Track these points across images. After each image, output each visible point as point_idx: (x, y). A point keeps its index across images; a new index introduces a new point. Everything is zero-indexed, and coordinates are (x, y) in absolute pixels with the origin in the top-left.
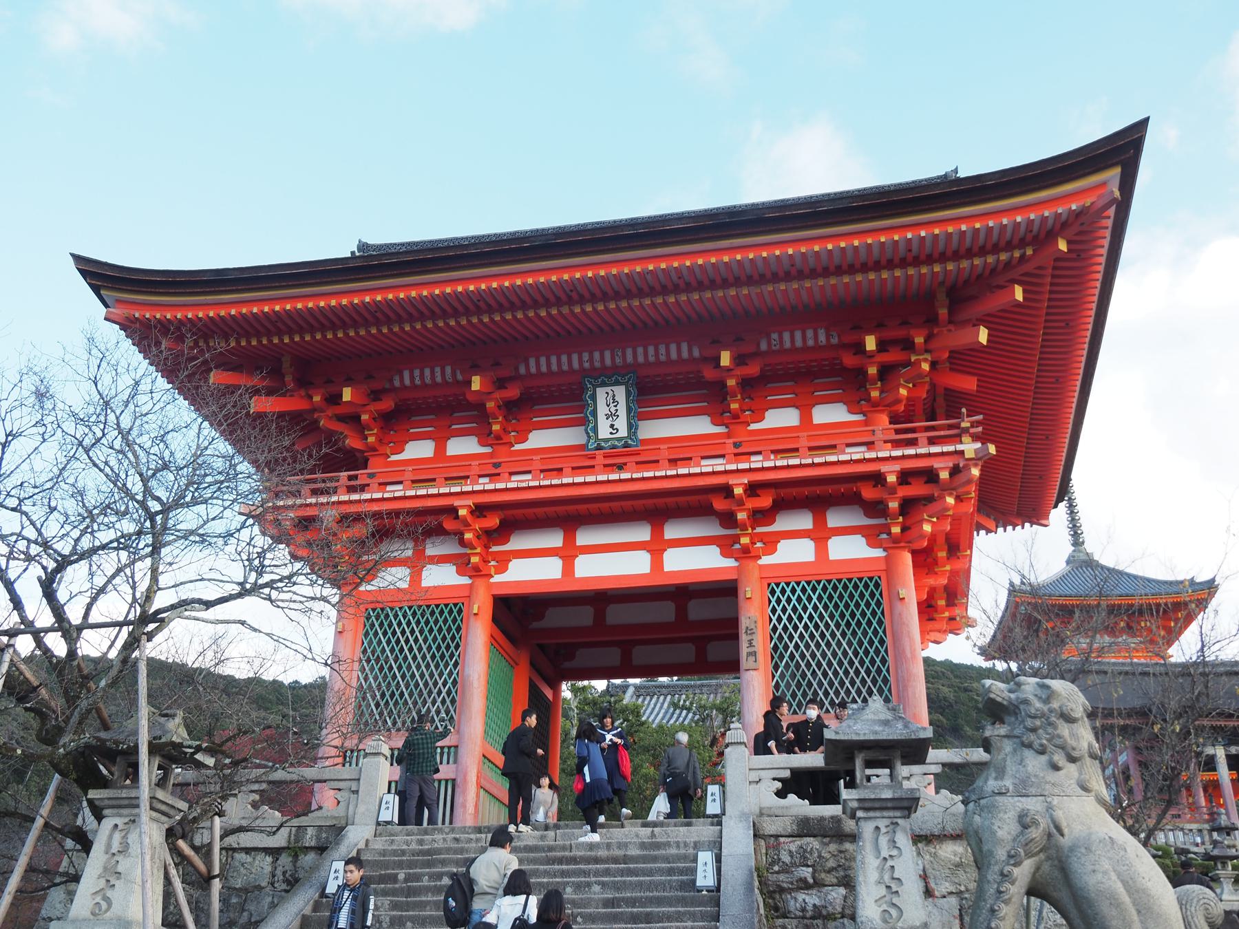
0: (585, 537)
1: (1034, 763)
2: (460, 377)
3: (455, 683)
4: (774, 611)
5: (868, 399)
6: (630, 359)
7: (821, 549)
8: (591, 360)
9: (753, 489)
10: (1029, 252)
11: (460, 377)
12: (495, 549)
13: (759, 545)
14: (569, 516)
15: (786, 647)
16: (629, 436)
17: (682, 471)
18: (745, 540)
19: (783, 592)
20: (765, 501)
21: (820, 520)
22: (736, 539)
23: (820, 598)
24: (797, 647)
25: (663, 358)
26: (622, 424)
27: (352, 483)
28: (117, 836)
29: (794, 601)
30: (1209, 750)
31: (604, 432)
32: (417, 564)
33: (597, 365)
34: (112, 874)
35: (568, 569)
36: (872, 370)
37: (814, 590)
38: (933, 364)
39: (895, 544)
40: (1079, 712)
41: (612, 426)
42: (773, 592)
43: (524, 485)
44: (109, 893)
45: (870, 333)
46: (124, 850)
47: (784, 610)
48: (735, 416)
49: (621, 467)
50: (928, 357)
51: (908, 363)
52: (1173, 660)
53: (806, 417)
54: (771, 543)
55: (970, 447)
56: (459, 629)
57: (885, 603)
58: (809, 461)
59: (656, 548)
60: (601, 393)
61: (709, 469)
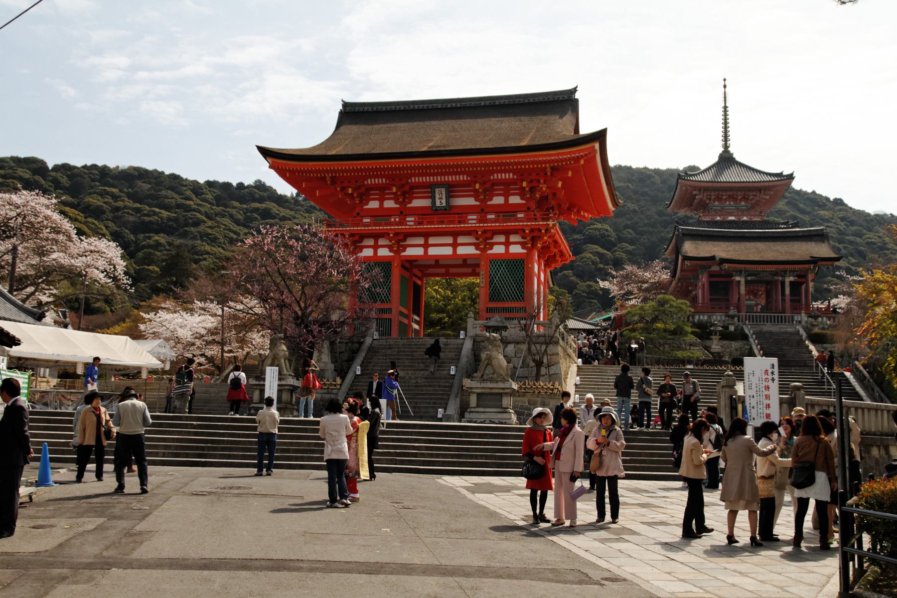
0: (432, 241)
1: (490, 347)
7: (507, 249)
9: (485, 232)
14: (426, 235)
20: (489, 235)
21: (507, 239)
26: (444, 201)
30: (738, 278)
31: (438, 204)
32: (376, 247)
34: (320, 352)
35: (426, 251)
38: (548, 187)
49: (442, 223)
54: (491, 246)
59: (455, 245)
60: (437, 190)
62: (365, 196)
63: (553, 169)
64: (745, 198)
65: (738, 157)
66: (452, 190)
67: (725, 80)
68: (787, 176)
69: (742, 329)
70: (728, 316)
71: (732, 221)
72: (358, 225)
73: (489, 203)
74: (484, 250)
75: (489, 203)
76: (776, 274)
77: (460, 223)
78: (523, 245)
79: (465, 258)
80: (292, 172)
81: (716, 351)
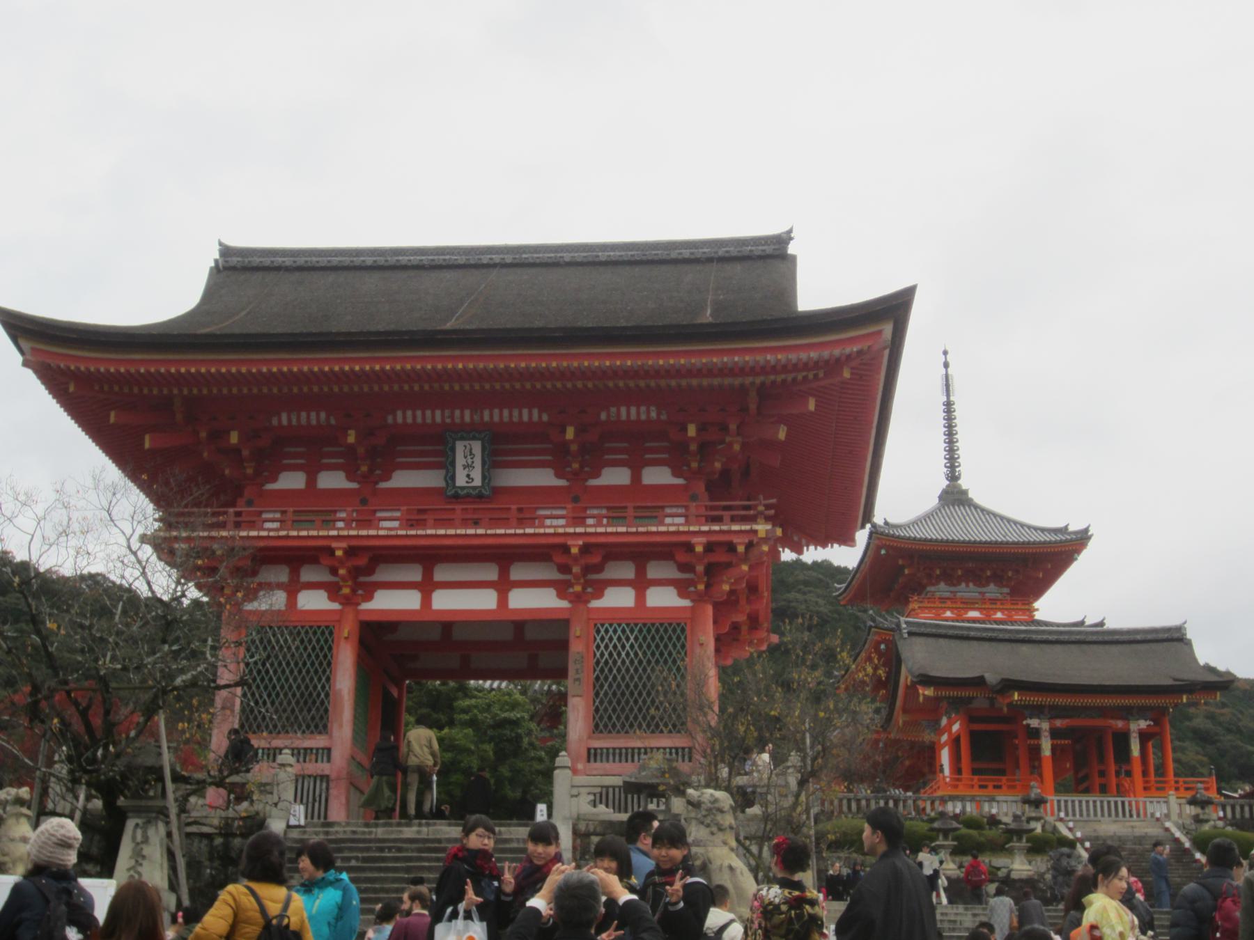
2: (333, 422)
3: (327, 695)
4: (598, 647)
5: (689, 465)
6: (486, 418)
7: (641, 598)
8: (452, 417)
9: (586, 549)
10: (821, 375)
11: (333, 422)
12: (362, 579)
13: (589, 590)
14: (429, 558)
15: (606, 678)
16: (483, 486)
17: (530, 531)
18: (578, 588)
19: (607, 631)
20: (595, 559)
21: (641, 571)
22: (568, 584)
23: (636, 639)
24: (615, 678)
25: (515, 419)
27: (239, 519)
28: (139, 832)
29: (615, 640)
30: (1034, 723)
31: (461, 480)
33: (457, 421)
35: (426, 601)
36: (693, 447)
37: (632, 631)
38: (744, 446)
39: (699, 599)
40: (727, 808)
41: (468, 476)
42: (598, 631)
43: (393, 533)
44: (139, 869)
45: (692, 422)
46: (146, 840)
47: (606, 647)
48: (576, 474)
49: (476, 523)
50: (740, 439)
51: (722, 442)
52: (1038, 616)
53: (636, 477)
54: (599, 589)
55: (762, 528)
56: (330, 649)
57: (688, 645)
58: (634, 530)
59: (503, 586)
60: (460, 447)
61: (551, 531)
62: (272, 456)
63: (765, 393)
64: (998, 579)
65: (976, 495)
66: (502, 447)
67: (945, 353)
68: (1075, 533)
69: (1055, 829)
70: (1026, 801)
71: (974, 620)
72: (252, 525)
73: (593, 482)
74: (579, 600)
75: (593, 482)
76: (1105, 712)
77: (521, 522)
78: (682, 588)
79: (521, 625)
80: (85, 379)
81: (1024, 875)
